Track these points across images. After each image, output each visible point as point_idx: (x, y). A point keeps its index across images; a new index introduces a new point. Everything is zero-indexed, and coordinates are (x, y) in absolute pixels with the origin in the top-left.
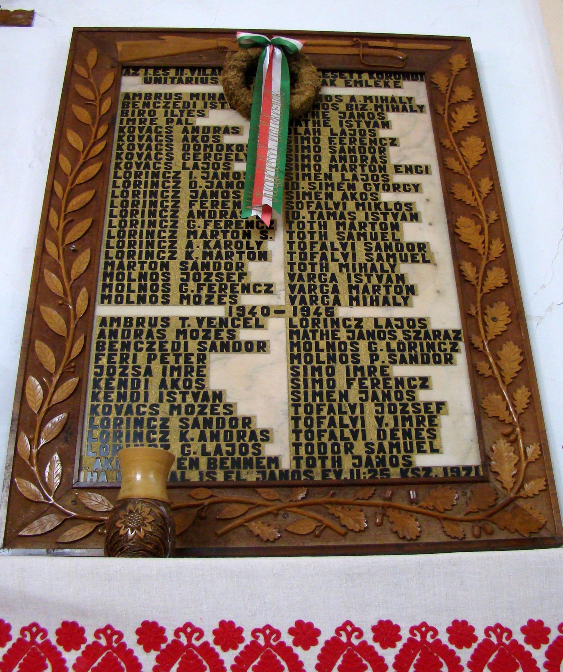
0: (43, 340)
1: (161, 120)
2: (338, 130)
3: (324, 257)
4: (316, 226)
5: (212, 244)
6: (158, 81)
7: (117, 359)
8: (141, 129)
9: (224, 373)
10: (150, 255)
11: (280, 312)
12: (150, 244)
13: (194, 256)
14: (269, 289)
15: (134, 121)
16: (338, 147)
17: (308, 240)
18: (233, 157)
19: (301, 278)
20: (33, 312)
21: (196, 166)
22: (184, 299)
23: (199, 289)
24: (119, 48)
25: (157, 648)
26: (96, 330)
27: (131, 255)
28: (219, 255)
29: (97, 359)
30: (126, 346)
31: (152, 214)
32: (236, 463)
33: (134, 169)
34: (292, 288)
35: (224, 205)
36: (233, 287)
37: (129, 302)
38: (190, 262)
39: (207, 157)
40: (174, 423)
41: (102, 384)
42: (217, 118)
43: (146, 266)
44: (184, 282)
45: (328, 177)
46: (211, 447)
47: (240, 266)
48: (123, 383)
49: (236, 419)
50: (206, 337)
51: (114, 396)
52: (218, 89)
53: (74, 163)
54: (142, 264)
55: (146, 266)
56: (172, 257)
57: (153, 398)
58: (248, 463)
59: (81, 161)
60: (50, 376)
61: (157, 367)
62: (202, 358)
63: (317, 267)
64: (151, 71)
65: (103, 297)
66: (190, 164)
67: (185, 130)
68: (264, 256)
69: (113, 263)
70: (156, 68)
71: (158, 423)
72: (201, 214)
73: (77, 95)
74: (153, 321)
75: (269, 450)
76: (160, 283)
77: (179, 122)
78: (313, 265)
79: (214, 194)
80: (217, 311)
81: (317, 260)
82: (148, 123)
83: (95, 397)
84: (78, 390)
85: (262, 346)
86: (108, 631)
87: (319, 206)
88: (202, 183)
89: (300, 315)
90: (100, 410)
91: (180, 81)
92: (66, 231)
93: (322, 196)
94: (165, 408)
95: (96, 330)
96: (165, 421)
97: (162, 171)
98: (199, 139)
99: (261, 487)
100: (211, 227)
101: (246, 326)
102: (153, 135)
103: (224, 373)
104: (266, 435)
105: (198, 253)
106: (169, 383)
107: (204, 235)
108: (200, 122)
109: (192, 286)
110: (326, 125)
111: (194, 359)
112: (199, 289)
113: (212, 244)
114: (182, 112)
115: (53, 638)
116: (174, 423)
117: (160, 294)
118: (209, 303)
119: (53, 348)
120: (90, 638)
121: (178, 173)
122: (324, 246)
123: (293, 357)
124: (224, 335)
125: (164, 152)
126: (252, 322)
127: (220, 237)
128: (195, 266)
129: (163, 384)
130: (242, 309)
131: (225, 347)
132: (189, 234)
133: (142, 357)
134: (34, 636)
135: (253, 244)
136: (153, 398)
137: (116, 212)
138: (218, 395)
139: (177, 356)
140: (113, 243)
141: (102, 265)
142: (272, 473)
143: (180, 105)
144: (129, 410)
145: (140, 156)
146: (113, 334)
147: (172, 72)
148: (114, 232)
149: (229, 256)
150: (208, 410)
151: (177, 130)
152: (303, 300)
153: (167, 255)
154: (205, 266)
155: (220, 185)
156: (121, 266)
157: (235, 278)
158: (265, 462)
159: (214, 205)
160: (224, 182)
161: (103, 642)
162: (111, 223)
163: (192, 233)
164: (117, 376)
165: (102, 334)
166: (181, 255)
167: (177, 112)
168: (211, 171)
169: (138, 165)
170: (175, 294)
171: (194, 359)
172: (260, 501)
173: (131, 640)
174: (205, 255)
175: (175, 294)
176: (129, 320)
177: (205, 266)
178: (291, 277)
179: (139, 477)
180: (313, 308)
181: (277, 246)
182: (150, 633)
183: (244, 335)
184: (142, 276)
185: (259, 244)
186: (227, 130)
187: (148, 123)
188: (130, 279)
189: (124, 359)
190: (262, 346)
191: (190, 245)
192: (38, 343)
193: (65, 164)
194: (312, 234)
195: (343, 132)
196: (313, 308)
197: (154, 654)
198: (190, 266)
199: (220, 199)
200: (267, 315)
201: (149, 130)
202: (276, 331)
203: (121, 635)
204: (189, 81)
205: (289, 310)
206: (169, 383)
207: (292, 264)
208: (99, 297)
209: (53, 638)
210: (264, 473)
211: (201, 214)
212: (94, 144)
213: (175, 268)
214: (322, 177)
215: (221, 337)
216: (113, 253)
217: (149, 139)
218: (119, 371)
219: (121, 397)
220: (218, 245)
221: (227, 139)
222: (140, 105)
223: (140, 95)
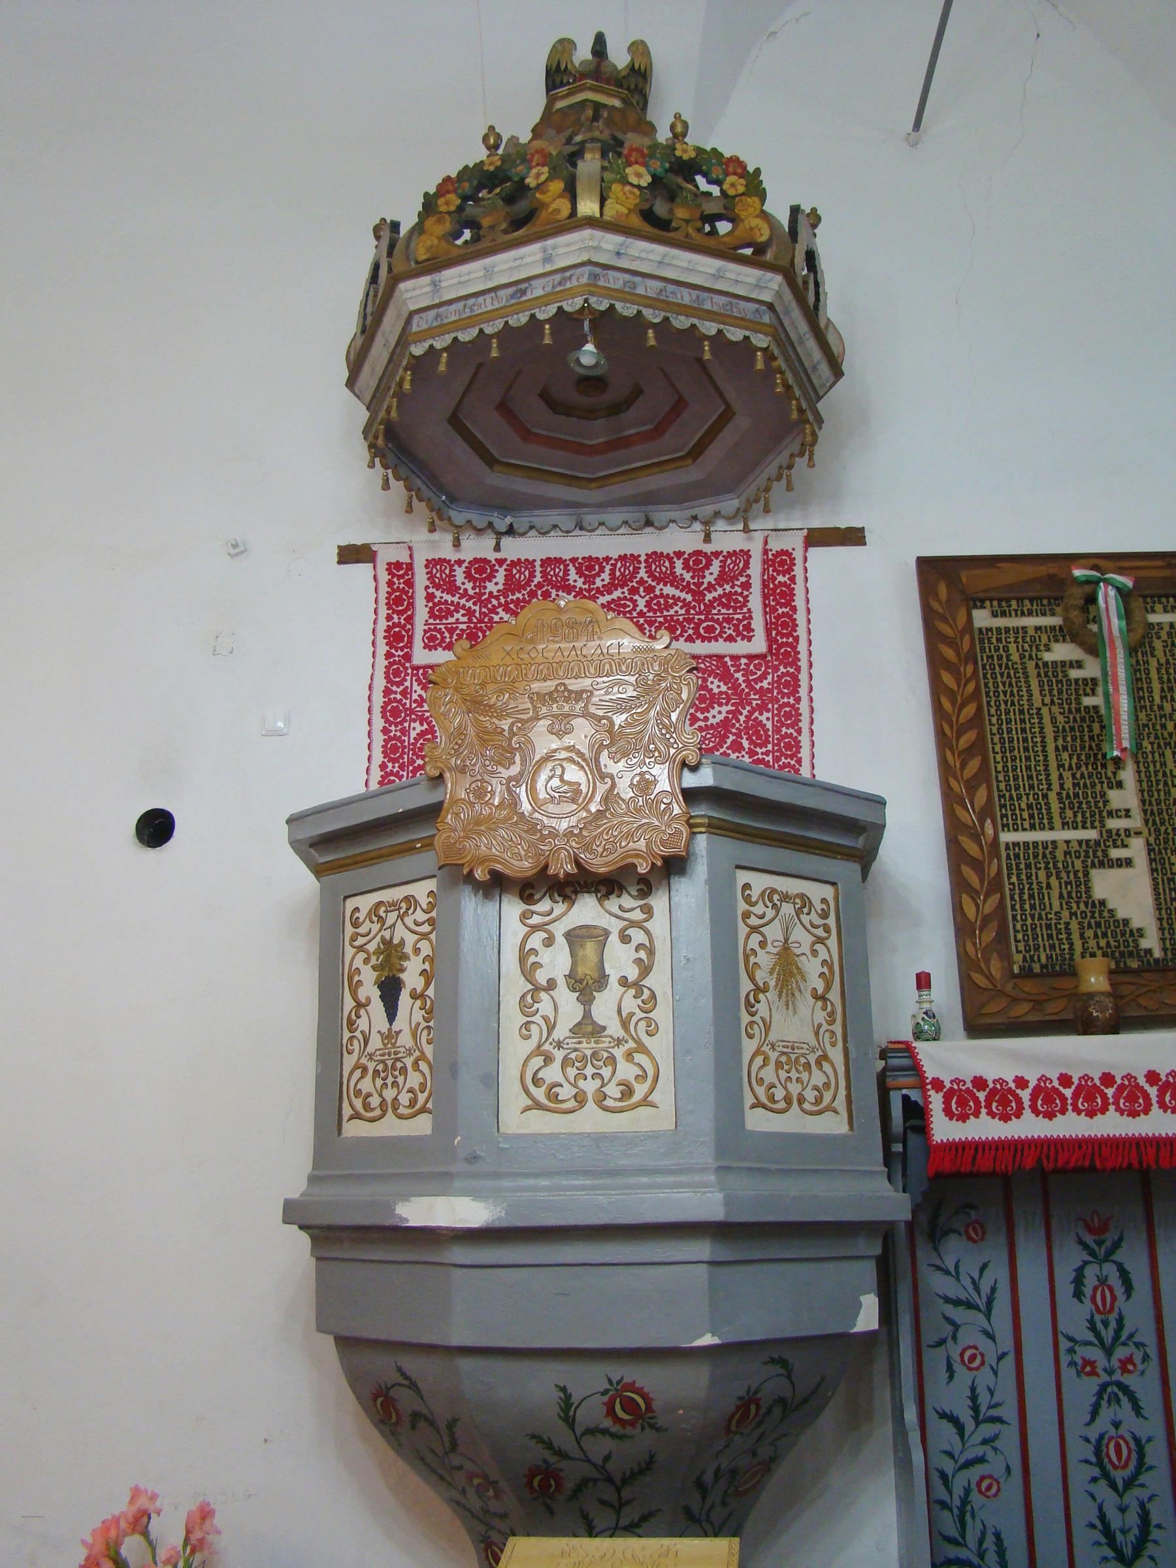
0: (967, 864)
1: (1015, 657)
2: (1163, 661)
3: (1166, 784)
4: (1156, 755)
5: (1078, 775)
6: (1003, 614)
7: (1023, 877)
8: (1000, 667)
9: (1104, 884)
10: (1031, 787)
11: (1138, 833)
12: (1030, 777)
13: (1066, 786)
14: (1128, 813)
15: (992, 657)
16: (1165, 677)
17: (1151, 768)
18: (1081, 692)
19: (1150, 804)
20: (952, 843)
21: (1052, 702)
22: (1065, 825)
23: (1075, 816)
24: (964, 579)
25: (1157, 1084)
26: (1004, 854)
27: (1017, 789)
28: (1085, 785)
29: (1009, 878)
30: (1028, 866)
31: (1026, 749)
32: (1122, 954)
33: (1003, 707)
34: (1145, 811)
35: (1082, 738)
36: (1100, 813)
37: (1024, 830)
38: (1064, 793)
39: (1060, 692)
40: (1074, 926)
41: (1017, 897)
42: (1062, 652)
43: (1031, 797)
44: (1063, 809)
45: (1161, 708)
46: (1103, 943)
47: (1103, 795)
48: (1031, 897)
49: (1118, 921)
50: (1087, 856)
51: (1027, 906)
52: (1056, 621)
53: (953, 703)
54: (1027, 795)
55: (1031, 797)
56: (1049, 789)
57: (1056, 907)
58: (1131, 954)
59: (959, 701)
60: (978, 893)
61: (1054, 881)
62: (1086, 874)
63: (1162, 793)
64: (995, 603)
65: (1003, 826)
66: (1047, 700)
67: (1037, 666)
68: (1120, 785)
69: (1004, 796)
70: (1000, 600)
71: (1062, 926)
72: (1065, 748)
73: (939, 632)
74: (1045, 845)
75: (1144, 944)
76: (1044, 812)
77: (1031, 658)
78: (1158, 791)
79: (1072, 729)
80: (1091, 834)
81: (1161, 787)
82: (1004, 659)
83: (1013, 909)
84: (1001, 904)
85: (1129, 862)
86: (1128, 1076)
87: (1156, 737)
88: (1060, 719)
89: (1153, 836)
90: (1019, 918)
91: (1023, 614)
92: (962, 768)
93: (1158, 727)
94: (1065, 914)
95: (1004, 854)
96: (1067, 924)
97: (1026, 707)
98: (1050, 674)
99: (1143, 971)
100: (1075, 760)
101: (1115, 846)
102: (1012, 672)
103: (1104, 884)
104: (1140, 932)
105: (1068, 784)
106: (1065, 894)
107: (1070, 768)
108: (1048, 657)
109: (1069, 813)
110: (1153, 656)
111: (1080, 875)
112: (1075, 816)
113: (1078, 775)
114: (1031, 646)
115: (1098, 1083)
116: (1074, 926)
117: (1045, 821)
118: (1084, 827)
119: (974, 870)
120: (1119, 1081)
121: (1039, 709)
122: (1165, 774)
123: (1153, 871)
124: (1100, 854)
125: (1024, 689)
126: (1119, 843)
127: (1083, 768)
128: (1068, 796)
129: (1061, 896)
130: (1109, 831)
131: (1102, 865)
132: (1059, 767)
133: (1042, 875)
134: (1086, 1081)
135: (1110, 774)
136: (1056, 907)
137: (997, 748)
138: (1103, 903)
139: (1068, 873)
140: (1001, 777)
141: (996, 799)
142: (1148, 961)
143: (1028, 639)
144: (1040, 918)
145: (1005, 693)
146: (1017, 856)
147: (1014, 603)
148: (1000, 768)
149: (1093, 786)
150: (1097, 915)
151: (1031, 666)
152: (1154, 822)
153: (1045, 787)
154: (1076, 795)
155: (1075, 720)
156: (1011, 798)
157: (1101, 805)
158: (1142, 953)
159: (1074, 739)
160: (1078, 716)
161: (1126, 1082)
162: (996, 760)
163: (1060, 766)
164: (1026, 891)
165: (1008, 857)
166: (1056, 786)
167: (1026, 646)
168: (1066, 706)
169: (1006, 702)
170: (1057, 821)
171: (1080, 875)
172: (1143, 982)
173: (1142, 1081)
174: (1075, 785)
175: (1057, 821)
176: (1026, 844)
177: (1076, 795)
178: (1143, 802)
179: (1093, 980)
180: (1163, 829)
181: (1128, 775)
182: (1152, 1077)
183: (1115, 853)
184: (1030, 806)
185: (1114, 774)
186: (1071, 666)
187: (1004, 659)
188: (1021, 810)
189: (1029, 877)
190: (1129, 862)
191: (1061, 777)
192: (963, 867)
193: (947, 705)
194: (1154, 762)
195: (1168, 662)
196: (1163, 829)
197: (1155, 1088)
198: (1064, 796)
199: (1078, 734)
200: (1129, 836)
201: (1007, 667)
202: (1137, 848)
203: (1136, 1078)
204: (1030, 614)
205: (1146, 832)
206: (1065, 894)
207: (1142, 791)
208: (1000, 826)
209: (1098, 1083)
210: (1143, 962)
211: (1065, 748)
212: (965, 685)
213: (1052, 796)
214: (1155, 708)
215: (1098, 855)
216: (1002, 786)
217: (1009, 676)
218: (1027, 886)
219: (1033, 907)
220: (1082, 776)
221: (1074, 674)
222: (994, 640)
223: (991, 629)
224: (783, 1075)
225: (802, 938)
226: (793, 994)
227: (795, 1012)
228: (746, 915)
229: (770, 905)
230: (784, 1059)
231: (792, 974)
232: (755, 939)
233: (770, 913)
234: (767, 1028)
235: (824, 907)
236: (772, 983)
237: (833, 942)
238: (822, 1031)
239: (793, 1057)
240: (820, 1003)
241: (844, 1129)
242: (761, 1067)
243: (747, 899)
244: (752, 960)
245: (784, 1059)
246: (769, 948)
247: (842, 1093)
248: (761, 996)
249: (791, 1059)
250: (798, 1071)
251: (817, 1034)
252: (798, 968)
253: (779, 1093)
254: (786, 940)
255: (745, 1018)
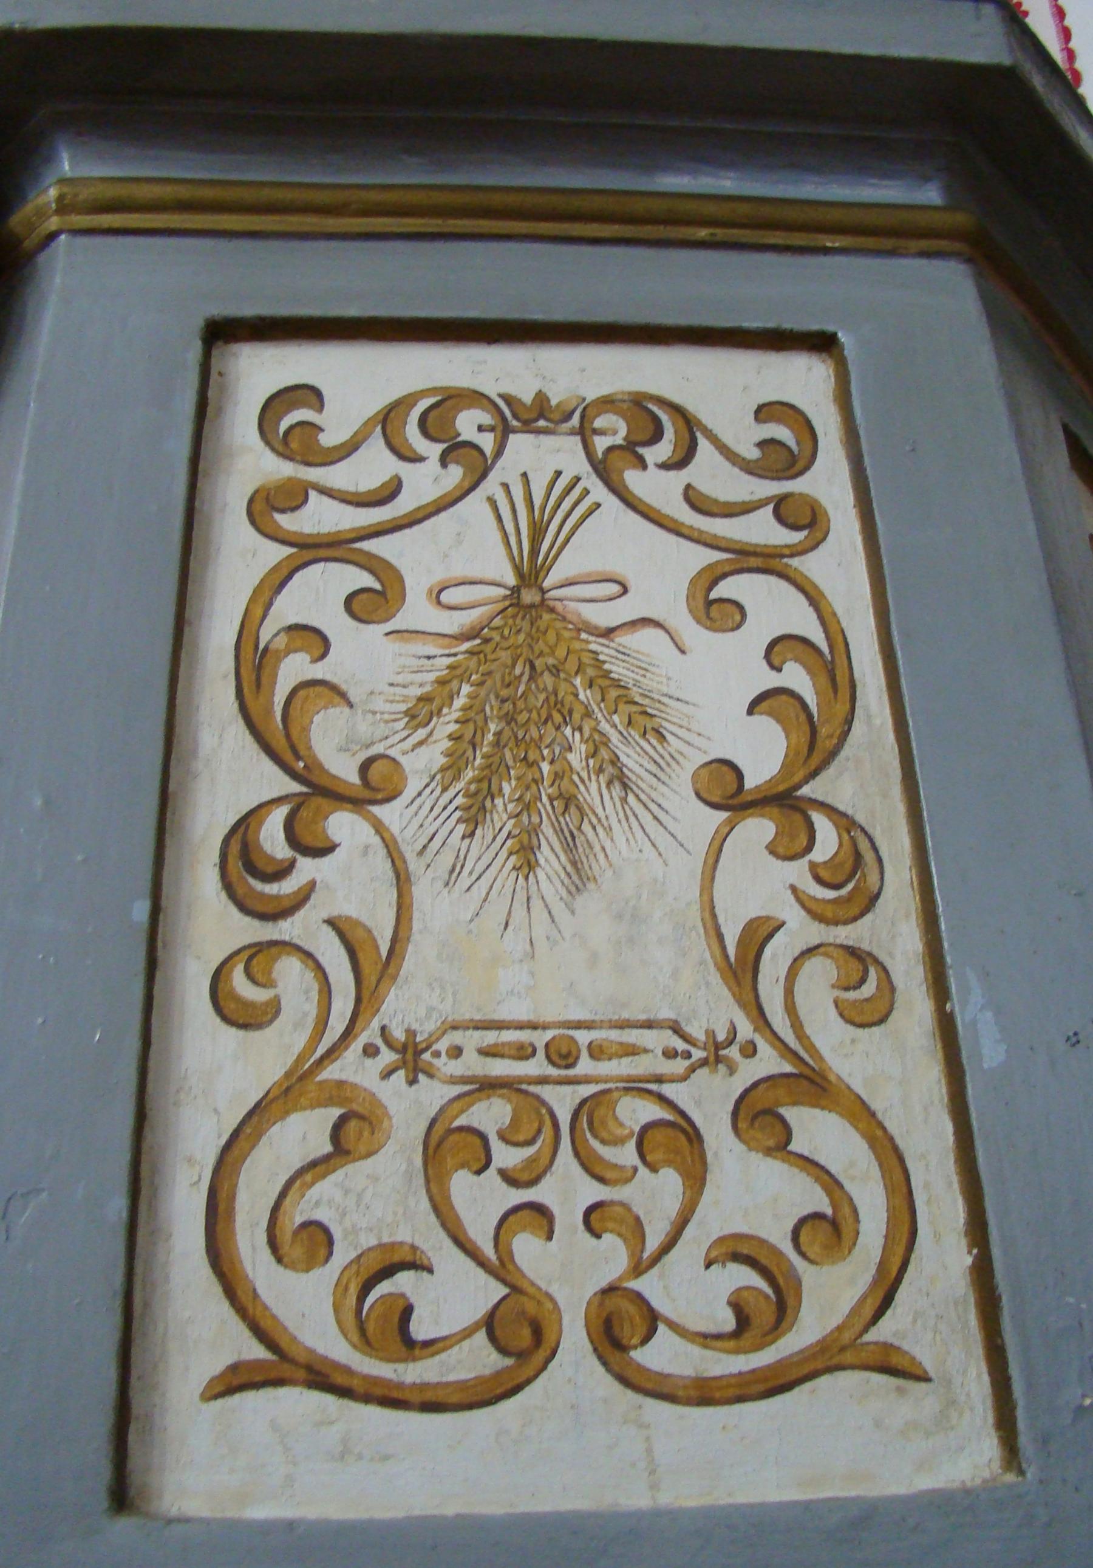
224: (480, 1200)
225: (626, 563)
226: (568, 801)
227: (579, 878)
228: (267, 506)
229: (433, 451)
230: (491, 1115)
231: (560, 711)
232: (319, 594)
233: (426, 480)
234: (375, 967)
235: (782, 433)
236: (422, 760)
237: (839, 566)
238: (776, 957)
239: (562, 1101)
240: (759, 829)
241: (970, 1457)
242: (316, 1168)
243: (299, 444)
244: (296, 667)
245: (491, 1115)
246: (416, 611)
247: (943, 1258)
248: (343, 826)
249: (546, 1105)
250: (593, 1168)
251: (742, 969)
252: (603, 681)
253: (450, 1298)
254: (530, 573)
255: (210, 925)
